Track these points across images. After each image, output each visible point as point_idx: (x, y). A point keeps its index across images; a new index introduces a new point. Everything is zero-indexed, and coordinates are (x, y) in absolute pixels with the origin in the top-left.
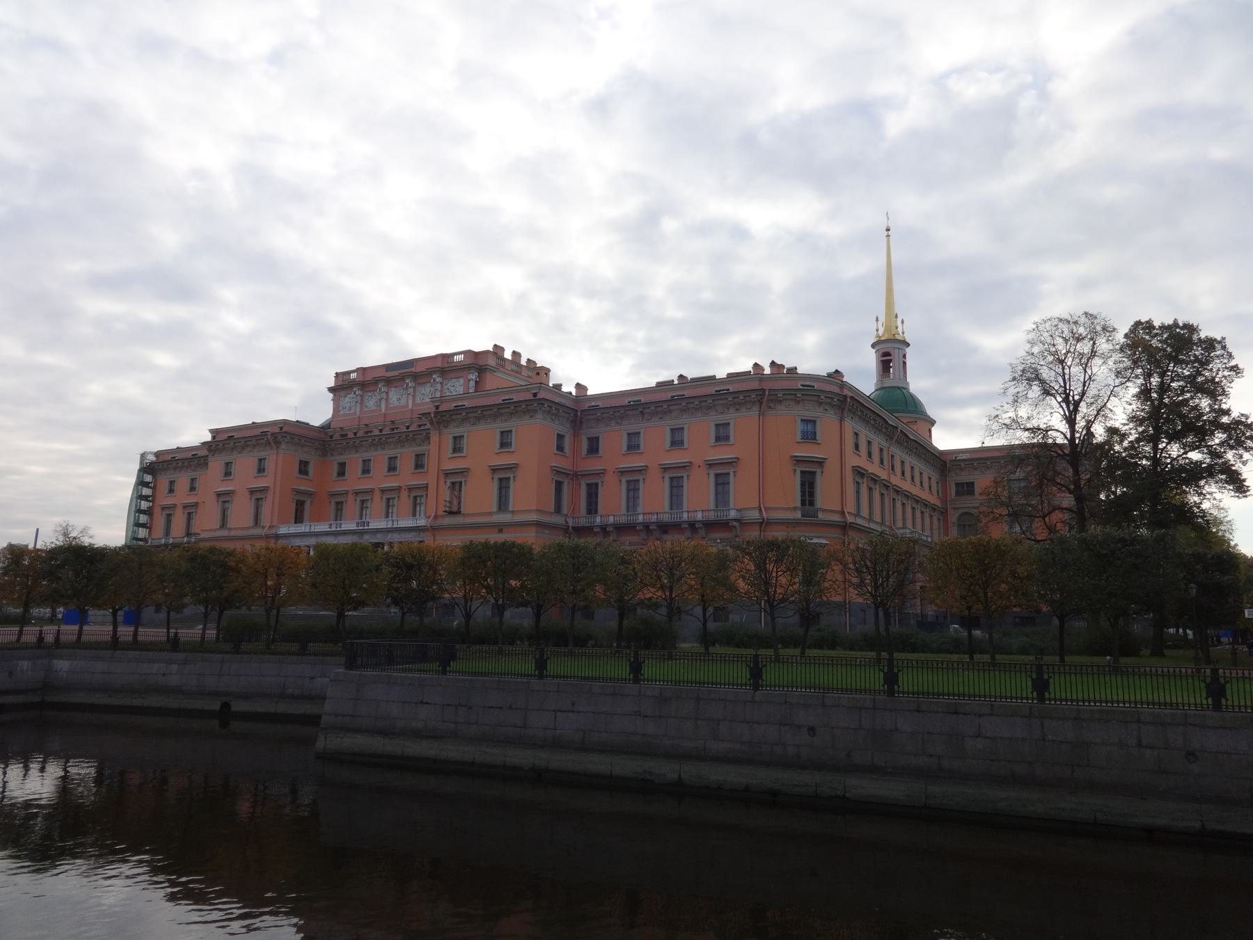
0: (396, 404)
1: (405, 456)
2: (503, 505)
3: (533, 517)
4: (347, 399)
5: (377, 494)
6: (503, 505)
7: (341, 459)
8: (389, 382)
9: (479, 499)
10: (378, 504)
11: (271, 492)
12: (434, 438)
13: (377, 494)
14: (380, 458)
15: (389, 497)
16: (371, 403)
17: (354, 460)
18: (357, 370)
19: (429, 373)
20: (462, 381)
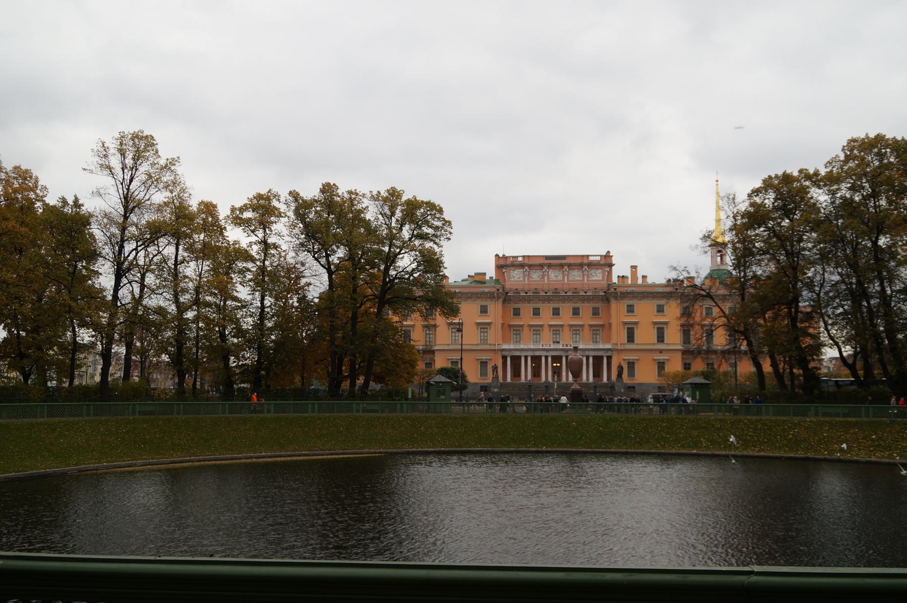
0: (555, 278)
1: (566, 309)
2: (661, 339)
3: (681, 348)
4: (516, 272)
5: (546, 329)
6: (661, 339)
7: (516, 306)
9: (645, 336)
10: (546, 334)
11: (493, 327)
12: (613, 303)
13: (546, 329)
14: (546, 310)
15: (556, 330)
16: (536, 275)
17: (527, 309)
18: (524, 257)
20: (600, 271)
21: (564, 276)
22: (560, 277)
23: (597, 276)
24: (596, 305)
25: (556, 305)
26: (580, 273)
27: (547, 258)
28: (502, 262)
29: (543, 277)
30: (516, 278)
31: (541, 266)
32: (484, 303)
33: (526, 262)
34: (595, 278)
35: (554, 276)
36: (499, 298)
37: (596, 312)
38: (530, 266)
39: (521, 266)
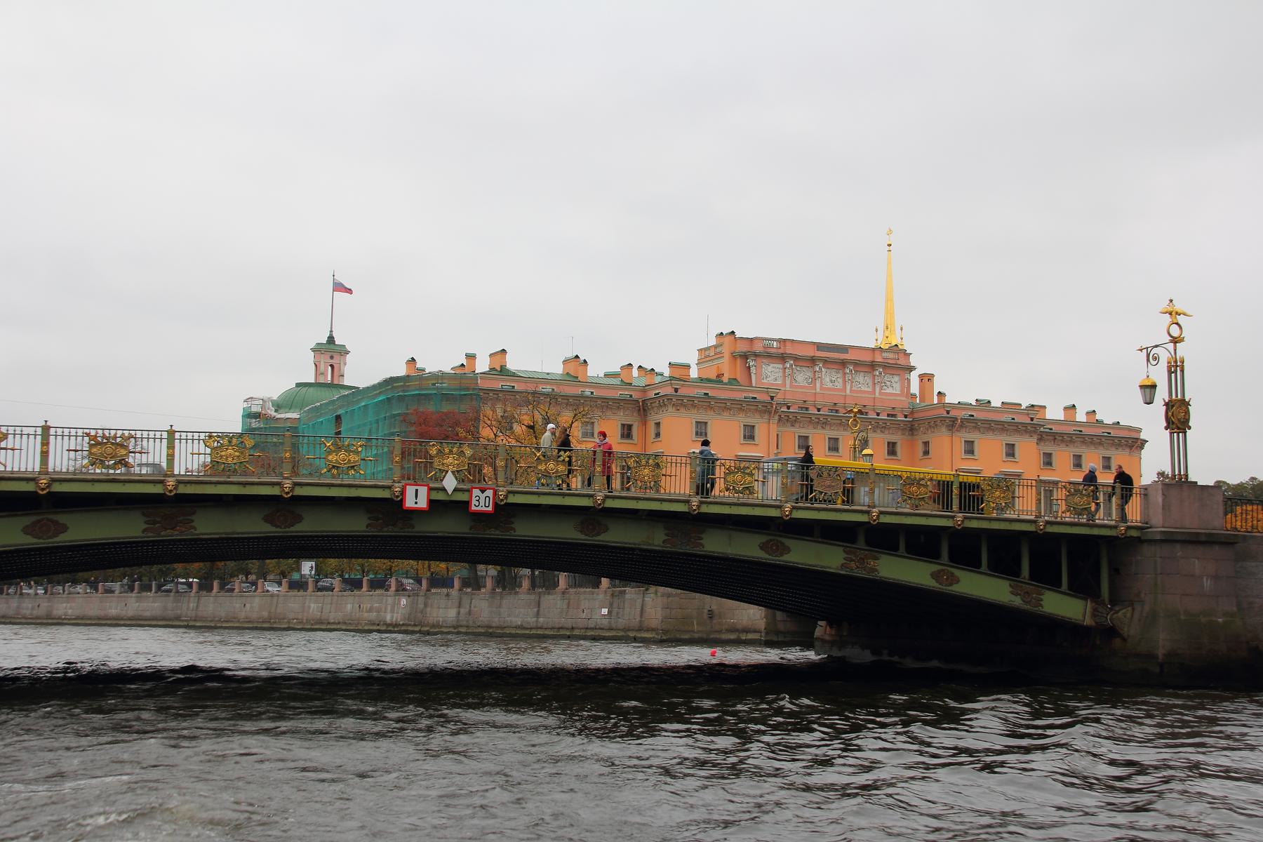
0: (830, 385)
4: (770, 368)
8: (826, 362)
16: (802, 376)
18: (783, 342)
19: (857, 364)
20: (896, 378)
21: (845, 382)
22: (839, 385)
23: (892, 386)
24: (893, 438)
25: (834, 434)
26: (869, 379)
27: (820, 346)
28: (742, 348)
29: (814, 379)
30: (770, 380)
31: (813, 361)
32: (750, 421)
33: (789, 350)
34: (889, 391)
35: (830, 383)
36: (776, 412)
37: (892, 449)
38: (796, 359)
39: (782, 358)
